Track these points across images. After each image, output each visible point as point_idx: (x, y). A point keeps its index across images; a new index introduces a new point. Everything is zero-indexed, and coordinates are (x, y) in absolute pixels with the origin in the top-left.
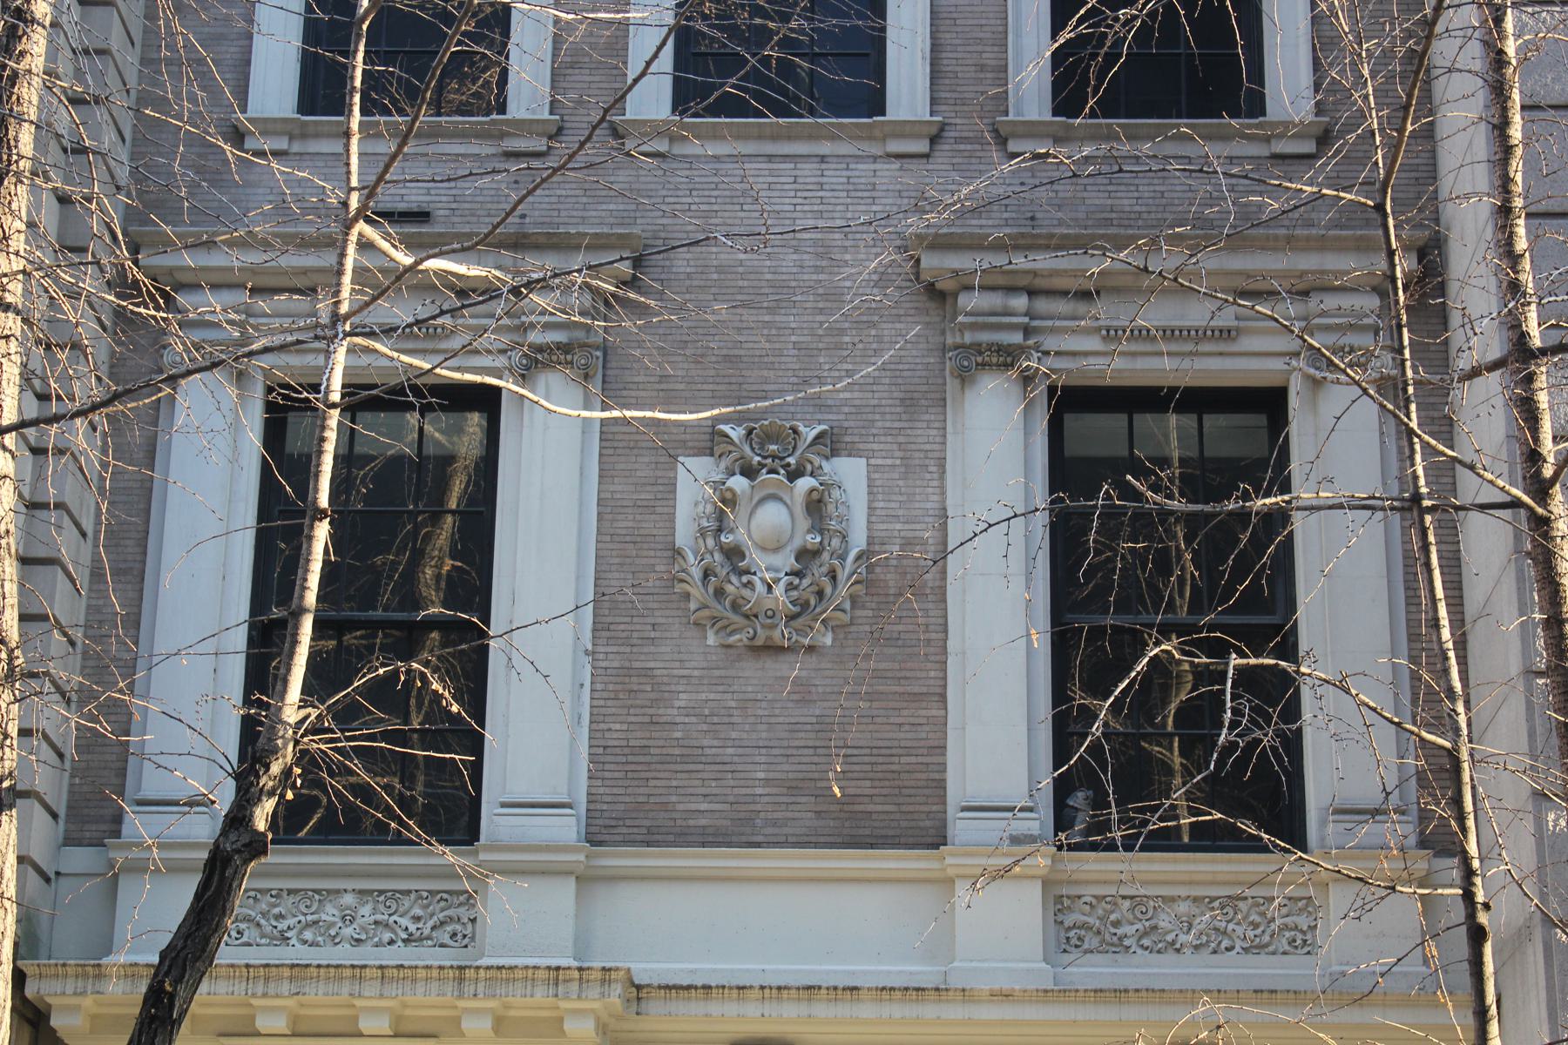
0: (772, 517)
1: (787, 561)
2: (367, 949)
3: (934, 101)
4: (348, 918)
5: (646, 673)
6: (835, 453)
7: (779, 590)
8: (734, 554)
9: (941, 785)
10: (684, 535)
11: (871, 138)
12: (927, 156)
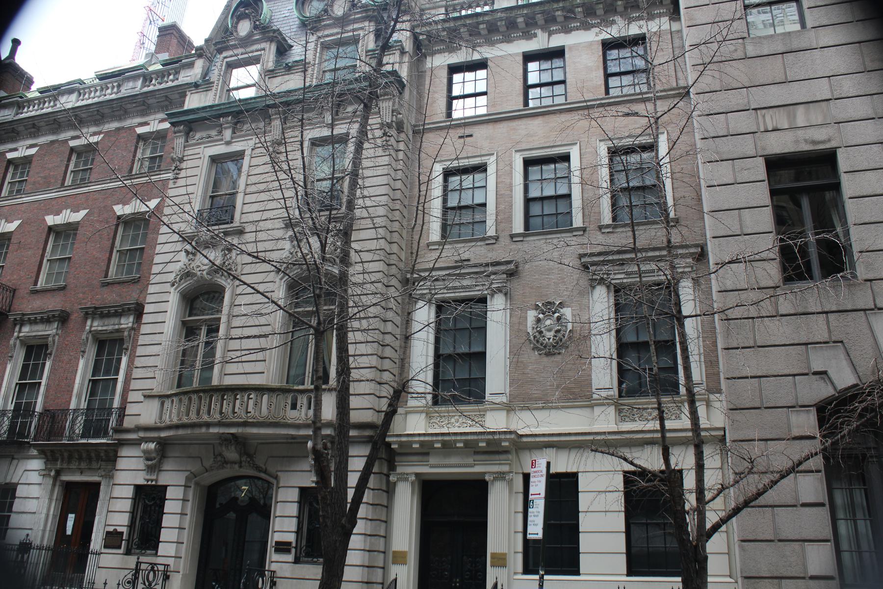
0: (548, 322)
1: (552, 333)
2: (461, 428)
3: (584, 222)
4: (457, 421)
5: (522, 362)
6: (564, 307)
7: (551, 340)
8: (541, 332)
9: (590, 385)
10: (530, 330)
11: (569, 232)
12: (582, 235)
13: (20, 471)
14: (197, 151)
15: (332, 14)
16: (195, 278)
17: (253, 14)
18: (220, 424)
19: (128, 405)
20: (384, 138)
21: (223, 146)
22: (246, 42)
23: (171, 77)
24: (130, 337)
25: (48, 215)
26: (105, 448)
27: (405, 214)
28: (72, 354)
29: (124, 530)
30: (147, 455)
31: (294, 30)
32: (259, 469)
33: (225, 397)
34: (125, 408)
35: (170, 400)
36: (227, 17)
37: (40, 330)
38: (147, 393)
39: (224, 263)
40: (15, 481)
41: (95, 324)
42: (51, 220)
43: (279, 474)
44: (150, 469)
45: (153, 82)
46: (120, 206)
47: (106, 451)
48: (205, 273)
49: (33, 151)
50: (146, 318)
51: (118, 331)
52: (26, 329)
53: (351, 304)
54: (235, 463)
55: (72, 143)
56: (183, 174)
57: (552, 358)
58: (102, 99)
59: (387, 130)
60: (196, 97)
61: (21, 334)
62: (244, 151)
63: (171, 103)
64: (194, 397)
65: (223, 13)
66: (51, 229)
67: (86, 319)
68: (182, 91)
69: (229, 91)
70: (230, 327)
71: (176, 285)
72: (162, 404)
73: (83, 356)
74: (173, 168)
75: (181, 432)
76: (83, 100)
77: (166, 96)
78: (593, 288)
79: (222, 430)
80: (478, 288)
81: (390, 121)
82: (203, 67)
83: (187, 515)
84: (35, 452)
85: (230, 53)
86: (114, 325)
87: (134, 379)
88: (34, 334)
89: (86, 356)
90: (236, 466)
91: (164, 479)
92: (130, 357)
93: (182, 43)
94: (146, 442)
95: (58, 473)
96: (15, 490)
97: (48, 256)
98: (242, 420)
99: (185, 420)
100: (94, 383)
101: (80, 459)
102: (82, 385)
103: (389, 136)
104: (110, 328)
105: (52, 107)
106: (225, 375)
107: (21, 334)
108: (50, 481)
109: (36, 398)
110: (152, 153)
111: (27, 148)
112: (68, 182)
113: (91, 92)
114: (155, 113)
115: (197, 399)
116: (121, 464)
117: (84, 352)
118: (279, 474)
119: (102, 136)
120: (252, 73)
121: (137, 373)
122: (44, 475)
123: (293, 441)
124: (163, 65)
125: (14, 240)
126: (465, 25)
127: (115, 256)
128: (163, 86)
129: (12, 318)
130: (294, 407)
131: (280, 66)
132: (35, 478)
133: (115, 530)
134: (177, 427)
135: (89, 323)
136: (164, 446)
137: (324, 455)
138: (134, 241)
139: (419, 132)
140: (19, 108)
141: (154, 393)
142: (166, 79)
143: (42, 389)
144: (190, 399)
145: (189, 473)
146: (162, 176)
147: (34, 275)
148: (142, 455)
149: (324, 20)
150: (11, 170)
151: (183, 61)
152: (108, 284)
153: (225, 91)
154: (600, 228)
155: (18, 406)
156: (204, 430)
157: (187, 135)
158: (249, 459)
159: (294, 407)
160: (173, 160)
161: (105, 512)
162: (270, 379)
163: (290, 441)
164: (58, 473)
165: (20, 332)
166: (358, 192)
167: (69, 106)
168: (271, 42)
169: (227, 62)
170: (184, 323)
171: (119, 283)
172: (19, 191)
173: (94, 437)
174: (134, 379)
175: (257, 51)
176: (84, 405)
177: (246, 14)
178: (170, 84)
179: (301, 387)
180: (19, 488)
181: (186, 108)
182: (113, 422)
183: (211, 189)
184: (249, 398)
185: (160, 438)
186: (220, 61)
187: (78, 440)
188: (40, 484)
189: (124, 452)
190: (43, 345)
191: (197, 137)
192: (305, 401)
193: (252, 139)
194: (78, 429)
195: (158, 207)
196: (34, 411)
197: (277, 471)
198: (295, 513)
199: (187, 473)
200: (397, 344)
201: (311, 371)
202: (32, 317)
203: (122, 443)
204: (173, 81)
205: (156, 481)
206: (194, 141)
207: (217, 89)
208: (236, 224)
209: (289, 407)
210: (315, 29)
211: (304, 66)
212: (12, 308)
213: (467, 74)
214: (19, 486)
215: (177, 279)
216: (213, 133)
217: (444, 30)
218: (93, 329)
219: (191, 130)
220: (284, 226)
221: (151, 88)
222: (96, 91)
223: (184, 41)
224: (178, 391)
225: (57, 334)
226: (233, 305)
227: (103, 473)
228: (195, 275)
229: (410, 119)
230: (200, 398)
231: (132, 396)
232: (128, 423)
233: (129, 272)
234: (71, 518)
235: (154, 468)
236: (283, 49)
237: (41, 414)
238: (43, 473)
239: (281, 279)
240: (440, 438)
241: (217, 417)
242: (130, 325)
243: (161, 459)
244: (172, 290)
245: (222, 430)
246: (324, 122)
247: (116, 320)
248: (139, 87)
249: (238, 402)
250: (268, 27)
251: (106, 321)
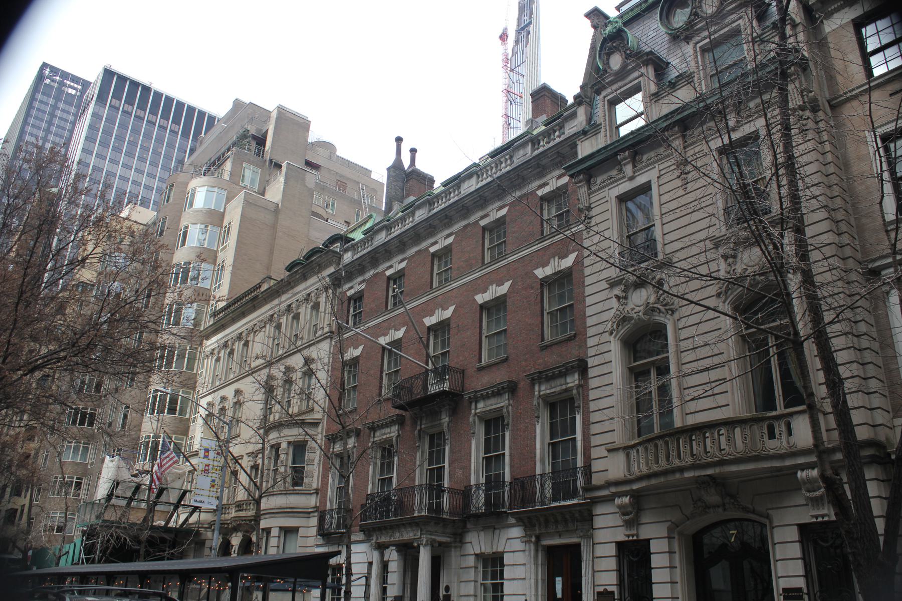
13: (503, 541)
14: (602, 195)
15: (703, 15)
16: (633, 322)
17: (622, 45)
18: (694, 467)
19: (593, 463)
21: (627, 183)
22: (622, 74)
23: (557, 134)
24: (579, 394)
25: (477, 294)
26: (578, 508)
27: (848, 199)
28: (527, 421)
29: (614, 589)
31: (666, 47)
32: (745, 509)
33: (694, 437)
34: (590, 466)
35: (635, 451)
36: (594, 59)
37: (494, 404)
38: (610, 446)
39: (659, 299)
40: (500, 549)
41: (543, 388)
42: (480, 299)
43: (770, 512)
44: (629, 524)
45: (542, 143)
46: (540, 269)
47: (580, 511)
48: (641, 314)
49: (450, 240)
50: (591, 373)
51: (566, 390)
52: (481, 405)
53: (824, 308)
54: (718, 507)
55: (483, 223)
56: (593, 222)
58: (499, 174)
59: (801, 113)
60: (587, 144)
61: (478, 411)
62: (650, 181)
63: (563, 157)
64: (660, 443)
65: (590, 56)
66: (482, 307)
67: (533, 385)
68: (571, 143)
69: (618, 127)
70: (680, 364)
71: (615, 333)
72: (628, 455)
73: (538, 422)
74: (583, 219)
75: (653, 482)
76: (482, 181)
77: (558, 152)
79: (698, 473)
81: (801, 103)
82: (586, 114)
83: (676, 567)
84: (512, 521)
85: (609, 90)
86: (561, 385)
87: (593, 435)
89: (540, 421)
90: (720, 510)
91: (645, 533)
92: (583, 414)
93: (556, 101)
94: (619, 497)
95: (538, 538)
96: (502, 559)
97: (485, 333)
98: (718, 459)
99: (655, 468)
100: (553, 445)
101: (556, 522)
102: (543, 449)
103: (805, 119)
104: (558, 389)
105: (457, 195)
106: (687, 414)
107: (478, 411)
108: (532, 547)
109: (504, 469)
110: (558, 210)
111: (445, 239)
112: (487, 259)
113: (488, 170)
114: (551, 172)
115: (663, 445)
116: (599, 522)
117: (538, 417)
118: (770, 512)
119: (507, 208)
120: (636, 103)
121: (594, 429)
122: (525, 542)
123: (778, 473)
124: (546, 125)
125: (453, 325)
127: (547, 318)
128: (552, 144)
129: (466, 397)
130: (772, 436)
131: (663, 86)
132: (518, 545)
133: (605, 590)
134: (648, 477)
135: (537, 388)
136: (638, 498)
137: (838, 482)
138: (561, 298)
139: (835, 105)
140: (430, 205)
141: (616, 445)
142: (552, 137)
143: (507, 459)
144: (656, 446)
145: (670, 523)
147: (477, 353)
148: (617, 510)
149: (696, 24)
150: (436, 262)
151: (565, 114)
152: (546, 347)
153: (614, 129)
155: (488, 478)
156: (678, 476)
157: (588, 183)
158: (732, 501)
159: (772, 436)
160: (581, 211)
161: (590, 572)
162: (737, 409)
163: (774, 474)
164: (538, 538)
165: (476, 408)
166: (800, 183)
167: (473, 189)
168: (647, 65)
169: (608, 100)
170: (631, 370)
171: (556, 344)
172: (446, 280)
173: (564, 499)
174: (593, 435)
175: (636, 79)
176: (548, 469)
177: (615, 47)
178: (558, 140)
179: (774, 413)
180: (506, 555)
181: (580, 157)
182: (580, 482)
183: (625, 230)
184: (719, 435)
185: (633, 491)
186: (600, 102)
187: (550, 504)
188: (524, 551)
189: (599, 509)
190: (498, 418)
191: (598, 182)
192: (783, 427)
193: (655, 167)
194: (548, 493)
195: (578, 262)
196: (504, 482)
197: (767, 509)
198: (799, 554)
200: (876, 346)
201: (781, 394)
202: (484, 393)
203: (595, 501)
204: (559, 136)
205: (637, 535)
206: (597, 187)
207: (606, 129)
208: (660, 257)
209: (766, 437)
210: (687, 39)
211: (686, 78)
212: (465, 388)
213: (879, 23)
214: (505, 554)
215: (615, 327)
216: (614, 173)
218: (542, 393)
219: (591, 177)
220: (712, 246)
221: (541, 149)
222: (492, 168)
223: (558, 99)
224: (641, 439)
225: (509, 405)
226: (678, 340)
227: (582, 534)
228: (631, 318)
229: (823, 96)
230: (667, 443)
231: (595, 453)
232: (596, 480)
233: (564, 331)
234: (559, 581)
235: (632, 523)
236: (660, 67)
237: (511, 483)
238: (524, 539)
239: (724, 302)
241: (689, 460)
242: (577, 382)
243: (637, 513)
244: (612, 338)
245: (698, 473)
247: (562, 381)
248: (530, 152)
249: (708, 441)
250: (640, 52)
251: (553, 383)
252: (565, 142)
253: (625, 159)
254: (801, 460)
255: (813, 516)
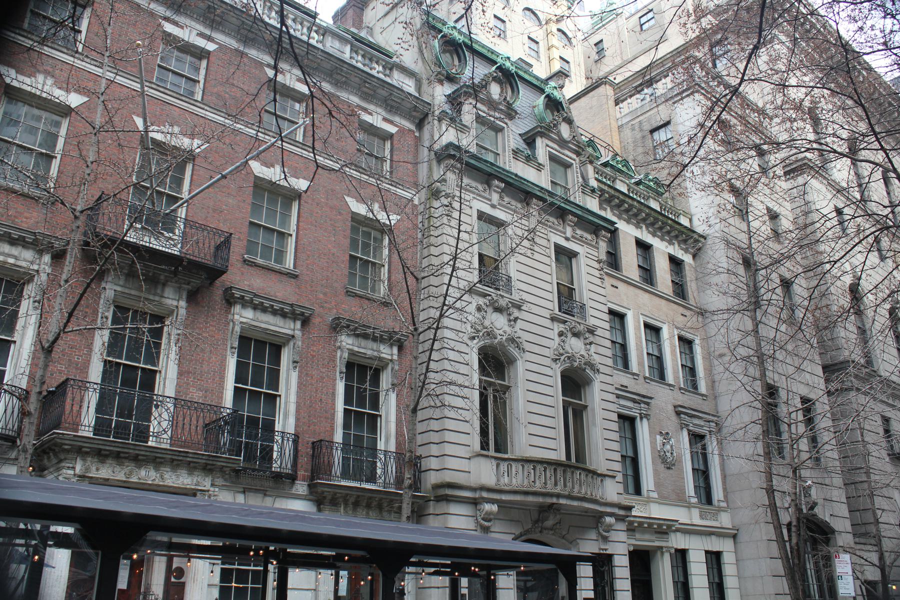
20: (602, 272)
30: (486, 516)
35: (506, 464)
43: (578, 541)
48: (504, 338)
57: (671, 471)
75: (530, 499)
78: (682, 428)
80: (634, 410)
88: (263, 326)
104: (369, 352)
126: (618, 198)
146: (398, 190)
154: (680, 389)
178: (374, 72)
199: (513, 536)
217: (608, 193)
240: (648, 521)
246: (565, 233)
247: (375, 345)
251: (363, 342)
252: (335, 61)
253: (498, 187)
254: (609, 510)
255: (600, 549)
